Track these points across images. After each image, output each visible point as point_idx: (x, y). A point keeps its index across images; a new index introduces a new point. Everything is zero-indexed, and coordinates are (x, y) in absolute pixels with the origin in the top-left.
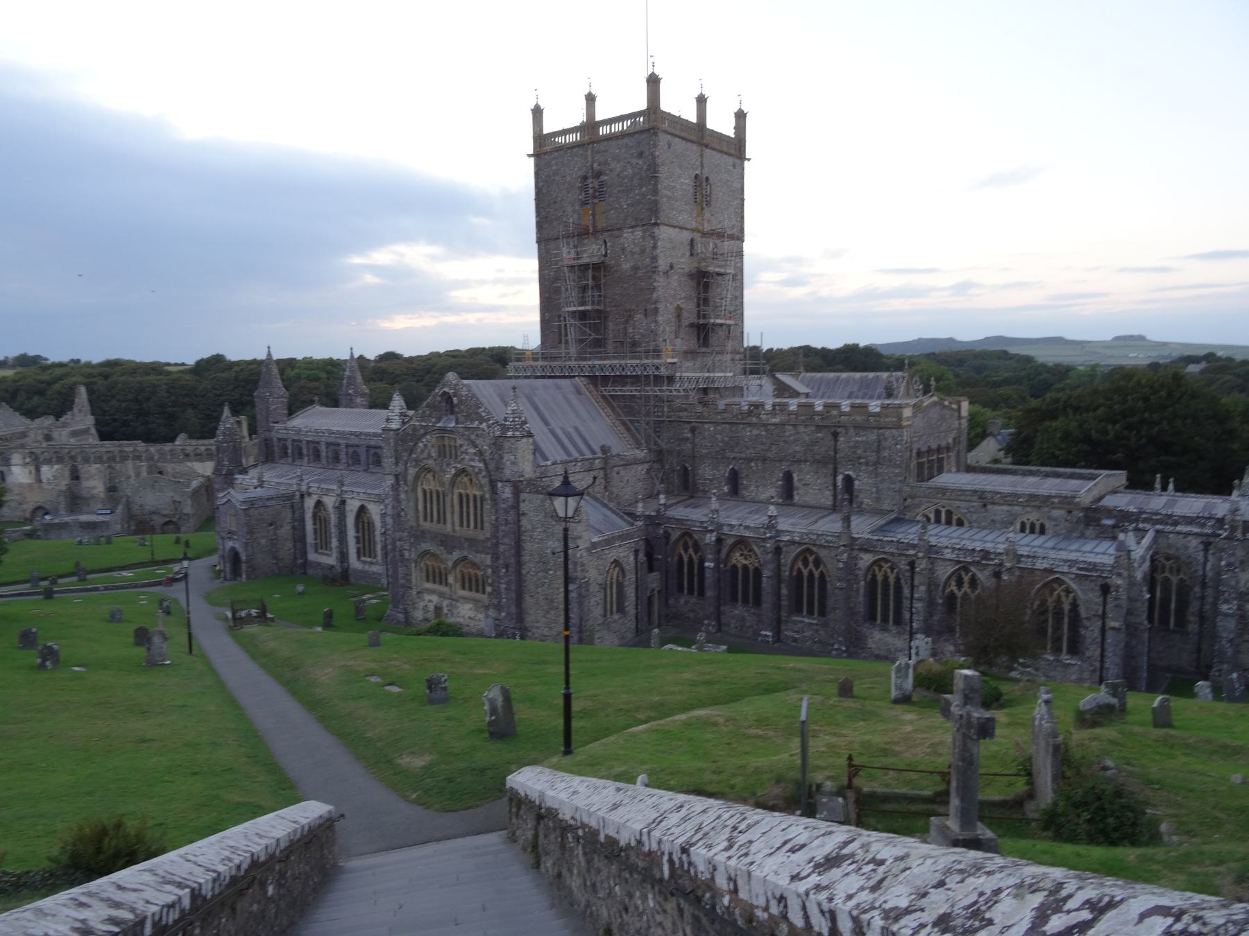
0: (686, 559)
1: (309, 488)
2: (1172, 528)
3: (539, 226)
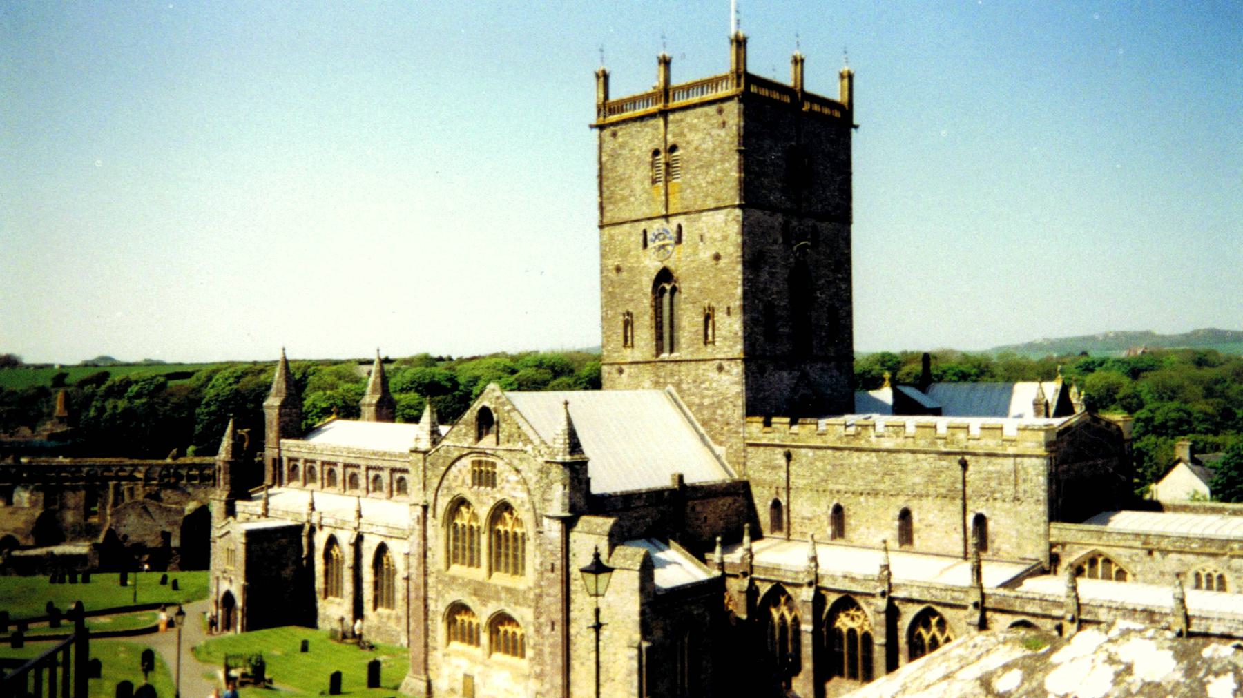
1: (321, 518)
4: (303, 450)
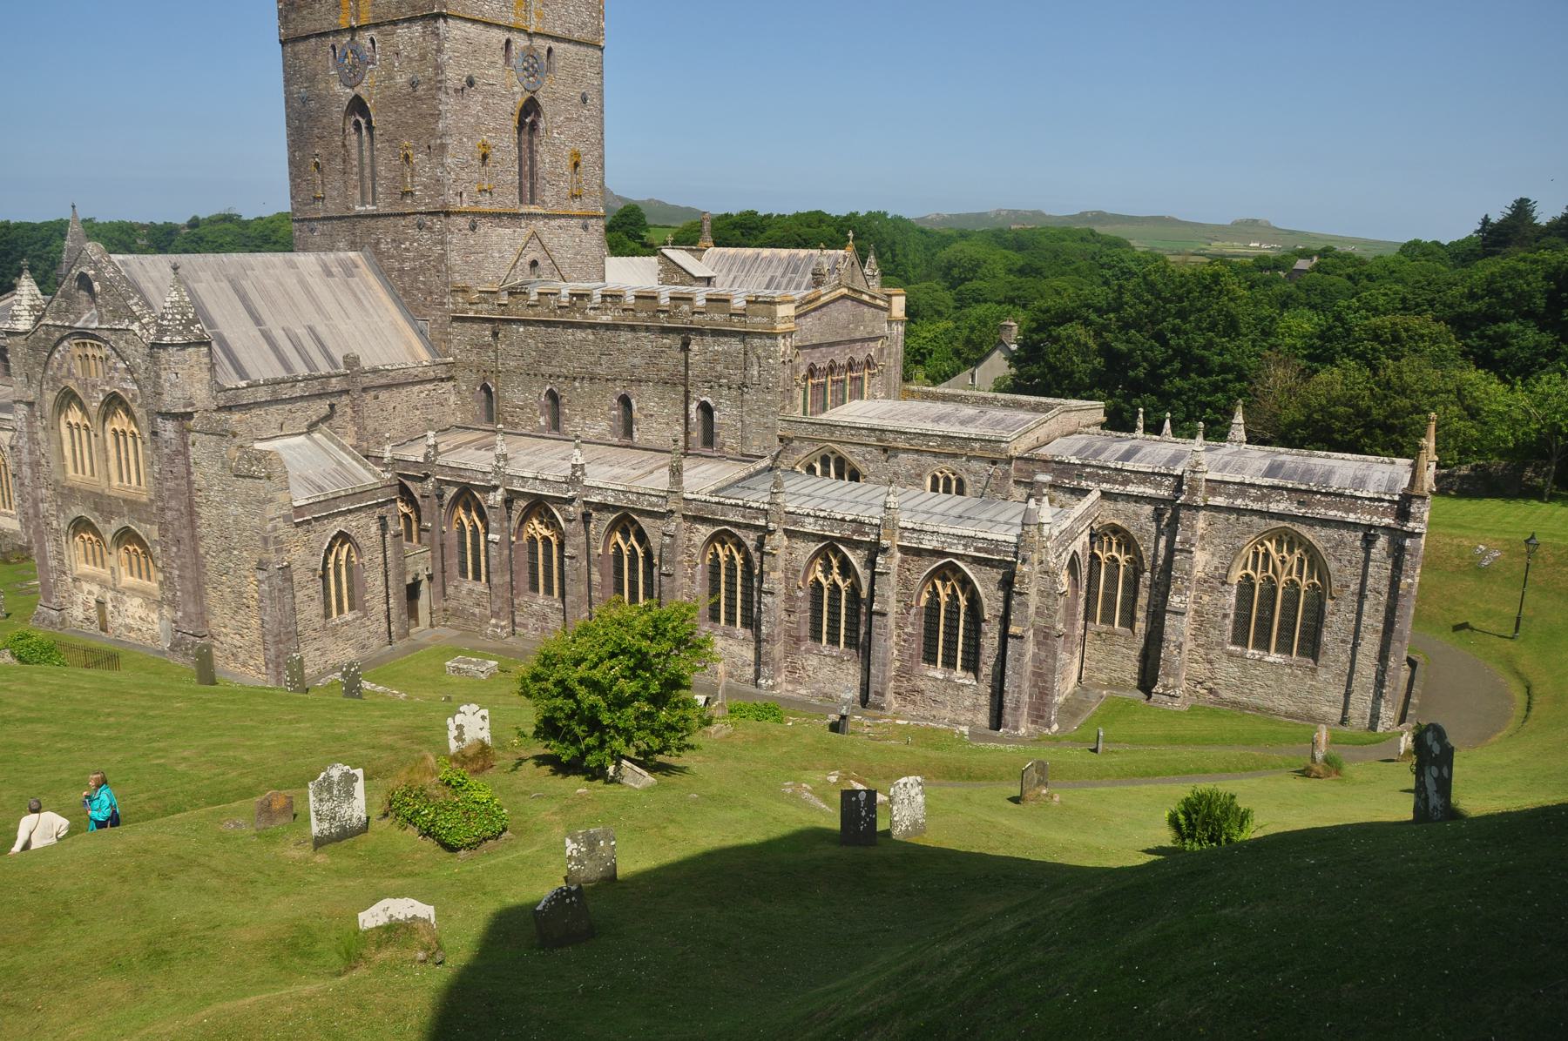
0: (468, 529)
2: (1122, 488)
3: (284, 17)
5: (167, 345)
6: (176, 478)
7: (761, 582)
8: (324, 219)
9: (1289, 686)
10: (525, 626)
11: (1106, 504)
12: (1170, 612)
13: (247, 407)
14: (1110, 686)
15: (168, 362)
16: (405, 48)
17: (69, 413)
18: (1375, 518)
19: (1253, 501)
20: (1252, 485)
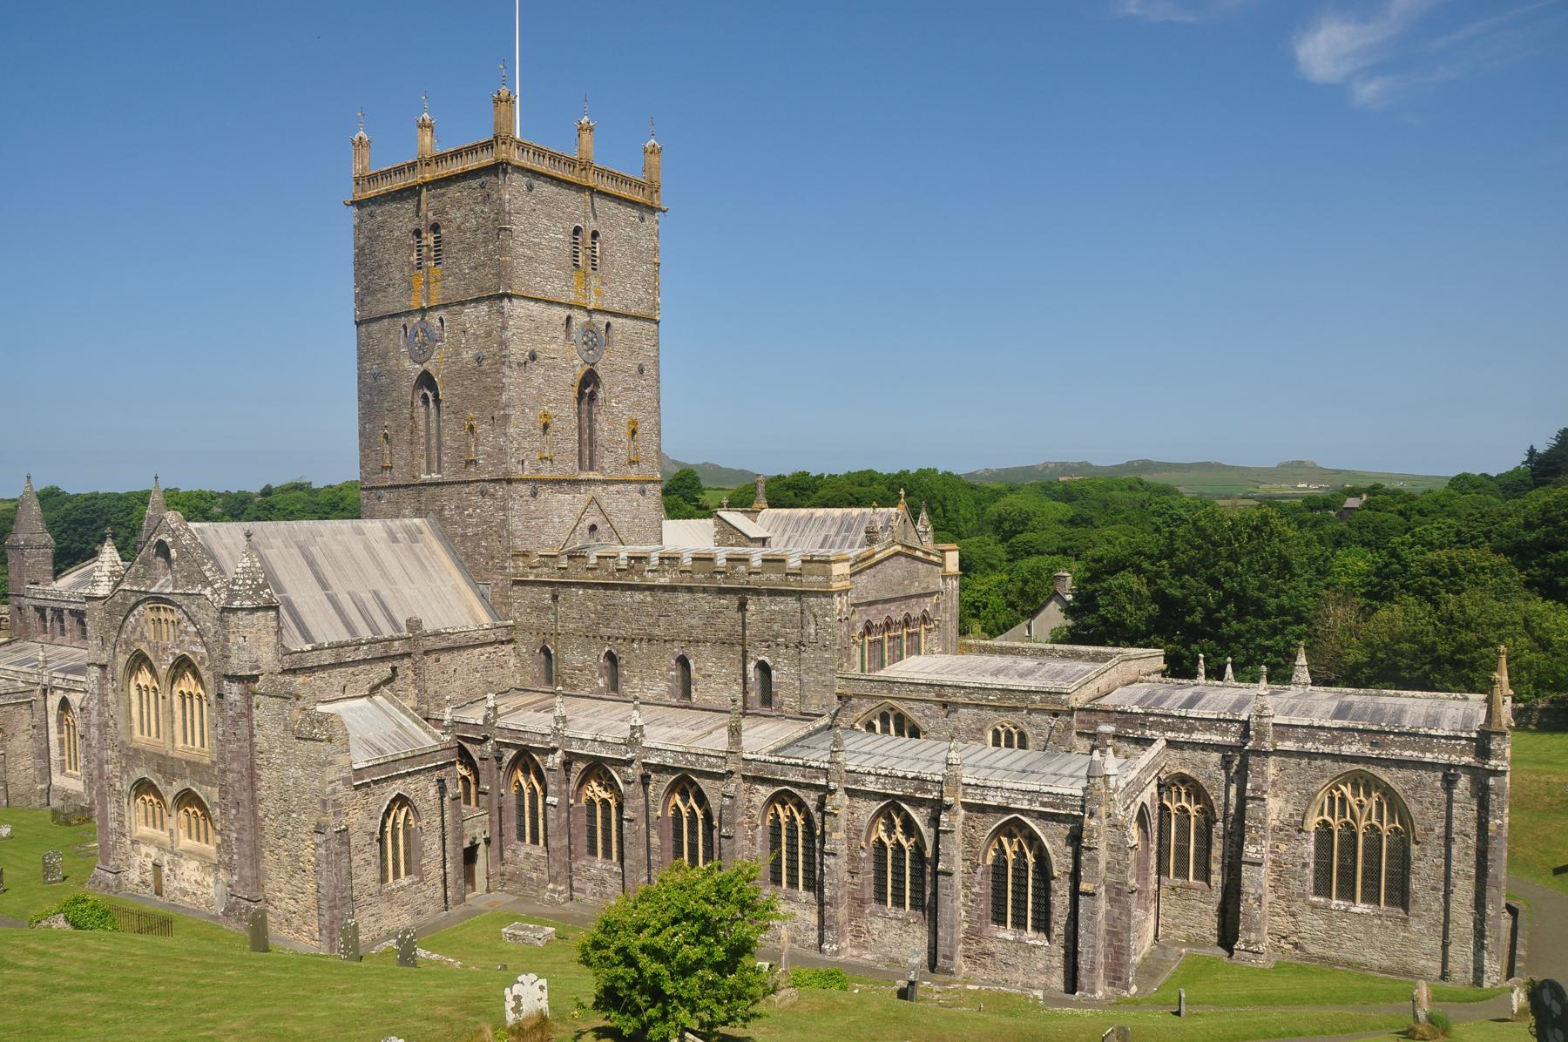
0: (527, 791)
2: (1187, 736)
3: (360, 300)
4: (49, 597)
5: (237, 609)
6: (239, 740)
7: (823, 843)
8: (391, 487)
9: (1380, 939)
10: (583, 891)
11: (1172, 753)
12: (1246, 863)
13: (312, 670)
14: (1189, 943)
15: (237, 625)
16: (472, 326)
17: (139, 675)
18: (1454, 757)
19: (1323, 744)
20: (1322, 728)
